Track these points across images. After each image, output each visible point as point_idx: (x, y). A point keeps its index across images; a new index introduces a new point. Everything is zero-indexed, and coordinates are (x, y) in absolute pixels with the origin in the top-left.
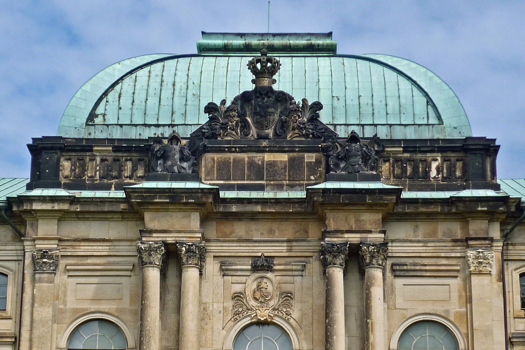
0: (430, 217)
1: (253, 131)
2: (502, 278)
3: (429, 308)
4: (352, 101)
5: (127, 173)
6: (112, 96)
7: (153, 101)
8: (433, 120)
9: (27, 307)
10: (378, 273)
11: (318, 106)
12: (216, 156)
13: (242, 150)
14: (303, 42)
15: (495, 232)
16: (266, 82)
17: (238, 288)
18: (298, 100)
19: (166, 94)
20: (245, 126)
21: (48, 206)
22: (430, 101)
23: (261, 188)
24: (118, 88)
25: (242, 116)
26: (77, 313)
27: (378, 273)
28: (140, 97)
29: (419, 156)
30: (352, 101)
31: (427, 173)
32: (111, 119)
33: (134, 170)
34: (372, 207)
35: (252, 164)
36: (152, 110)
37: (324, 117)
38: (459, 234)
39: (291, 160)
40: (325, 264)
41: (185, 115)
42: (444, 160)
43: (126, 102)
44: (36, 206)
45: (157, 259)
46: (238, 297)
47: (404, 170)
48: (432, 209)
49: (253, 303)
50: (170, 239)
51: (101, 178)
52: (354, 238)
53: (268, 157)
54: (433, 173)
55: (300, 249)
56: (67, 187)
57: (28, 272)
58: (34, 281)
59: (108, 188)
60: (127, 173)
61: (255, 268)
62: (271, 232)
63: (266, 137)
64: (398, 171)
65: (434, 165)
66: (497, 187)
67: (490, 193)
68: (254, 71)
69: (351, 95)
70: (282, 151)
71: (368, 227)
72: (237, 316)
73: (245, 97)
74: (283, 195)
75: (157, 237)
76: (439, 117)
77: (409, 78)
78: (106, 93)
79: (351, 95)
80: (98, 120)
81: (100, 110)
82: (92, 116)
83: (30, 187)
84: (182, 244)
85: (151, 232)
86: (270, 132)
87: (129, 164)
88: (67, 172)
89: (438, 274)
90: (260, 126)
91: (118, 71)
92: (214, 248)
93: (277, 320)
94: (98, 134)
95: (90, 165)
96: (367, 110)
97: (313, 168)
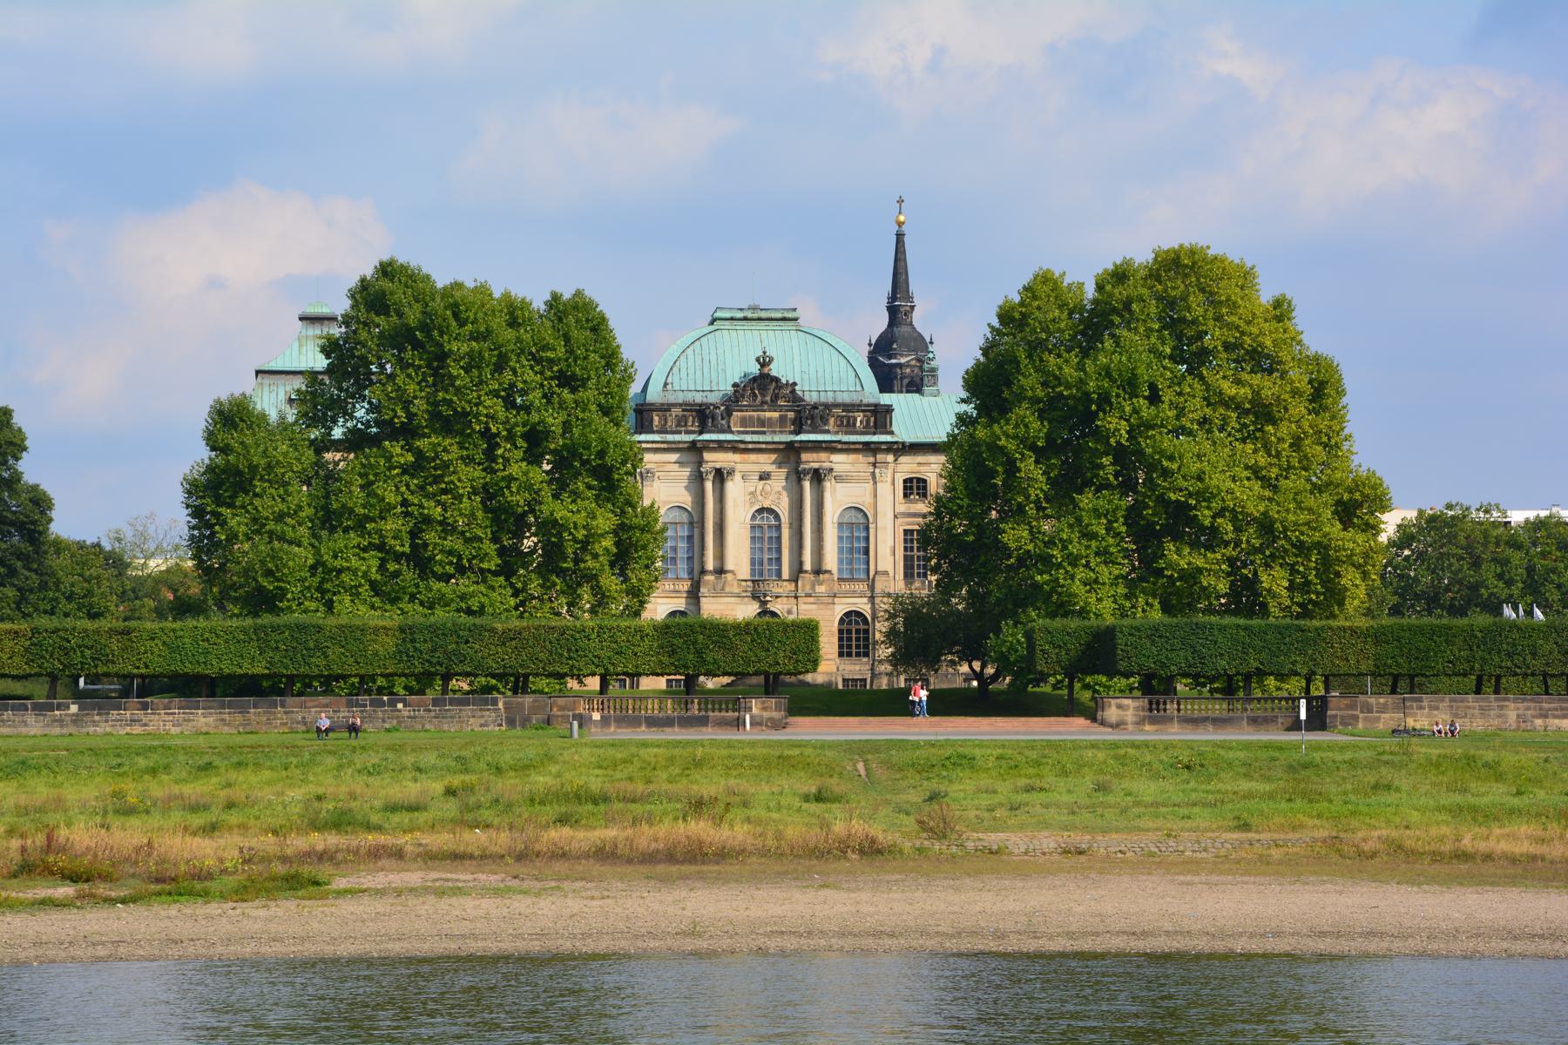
0: (856, 451)
1: (759, 398)
4: (813, 376)
5: (690, 424)
7: (699, 373)
8: (859, 388)
11: (795, 384)
13: (753, 411)
16: (766, 370)
17: (753, 489)
18: (784, 381)
20: (755, 395)
22: (857, 375)
23: (764, 433)
24: (678, 363)
25: (752, 389)
29: (851, 414)
31: (854, 424)
33: (693, 422)
35: (759, 418)
37: (797, 388)
39: (781, 417)
42: (864, 416)
44: (644, 445)
45: (711, 477)
46: (752, 493)
47: (842, 422)
48: (857, 446)
49: (760, 498)
51: (676, 426)
52: (816, 465)
53: (768, 414)
54: (858, 424)
56: (659, 432)
59: (680, 433)
60: (690, 424)
61: (761, 478)
63: (766, 403)
64: (839, 423)
65: (859, 419)
66: (892, 433)
67: (888, 438)
68: (759, 363)
69: (812, 372)
70: (775, 411)
72: (752, 504)
73: (755, 379)
74: (777, 438)
75: (710, 465)
78: (671, 369)
80: (669, 387)
81: (669, 380)
82: (666, 384)
86: (768, 398)
90: (763, 395)
91: (675, 350)
94: (671, 399)
95: (669, 419)
96: (821, 380)
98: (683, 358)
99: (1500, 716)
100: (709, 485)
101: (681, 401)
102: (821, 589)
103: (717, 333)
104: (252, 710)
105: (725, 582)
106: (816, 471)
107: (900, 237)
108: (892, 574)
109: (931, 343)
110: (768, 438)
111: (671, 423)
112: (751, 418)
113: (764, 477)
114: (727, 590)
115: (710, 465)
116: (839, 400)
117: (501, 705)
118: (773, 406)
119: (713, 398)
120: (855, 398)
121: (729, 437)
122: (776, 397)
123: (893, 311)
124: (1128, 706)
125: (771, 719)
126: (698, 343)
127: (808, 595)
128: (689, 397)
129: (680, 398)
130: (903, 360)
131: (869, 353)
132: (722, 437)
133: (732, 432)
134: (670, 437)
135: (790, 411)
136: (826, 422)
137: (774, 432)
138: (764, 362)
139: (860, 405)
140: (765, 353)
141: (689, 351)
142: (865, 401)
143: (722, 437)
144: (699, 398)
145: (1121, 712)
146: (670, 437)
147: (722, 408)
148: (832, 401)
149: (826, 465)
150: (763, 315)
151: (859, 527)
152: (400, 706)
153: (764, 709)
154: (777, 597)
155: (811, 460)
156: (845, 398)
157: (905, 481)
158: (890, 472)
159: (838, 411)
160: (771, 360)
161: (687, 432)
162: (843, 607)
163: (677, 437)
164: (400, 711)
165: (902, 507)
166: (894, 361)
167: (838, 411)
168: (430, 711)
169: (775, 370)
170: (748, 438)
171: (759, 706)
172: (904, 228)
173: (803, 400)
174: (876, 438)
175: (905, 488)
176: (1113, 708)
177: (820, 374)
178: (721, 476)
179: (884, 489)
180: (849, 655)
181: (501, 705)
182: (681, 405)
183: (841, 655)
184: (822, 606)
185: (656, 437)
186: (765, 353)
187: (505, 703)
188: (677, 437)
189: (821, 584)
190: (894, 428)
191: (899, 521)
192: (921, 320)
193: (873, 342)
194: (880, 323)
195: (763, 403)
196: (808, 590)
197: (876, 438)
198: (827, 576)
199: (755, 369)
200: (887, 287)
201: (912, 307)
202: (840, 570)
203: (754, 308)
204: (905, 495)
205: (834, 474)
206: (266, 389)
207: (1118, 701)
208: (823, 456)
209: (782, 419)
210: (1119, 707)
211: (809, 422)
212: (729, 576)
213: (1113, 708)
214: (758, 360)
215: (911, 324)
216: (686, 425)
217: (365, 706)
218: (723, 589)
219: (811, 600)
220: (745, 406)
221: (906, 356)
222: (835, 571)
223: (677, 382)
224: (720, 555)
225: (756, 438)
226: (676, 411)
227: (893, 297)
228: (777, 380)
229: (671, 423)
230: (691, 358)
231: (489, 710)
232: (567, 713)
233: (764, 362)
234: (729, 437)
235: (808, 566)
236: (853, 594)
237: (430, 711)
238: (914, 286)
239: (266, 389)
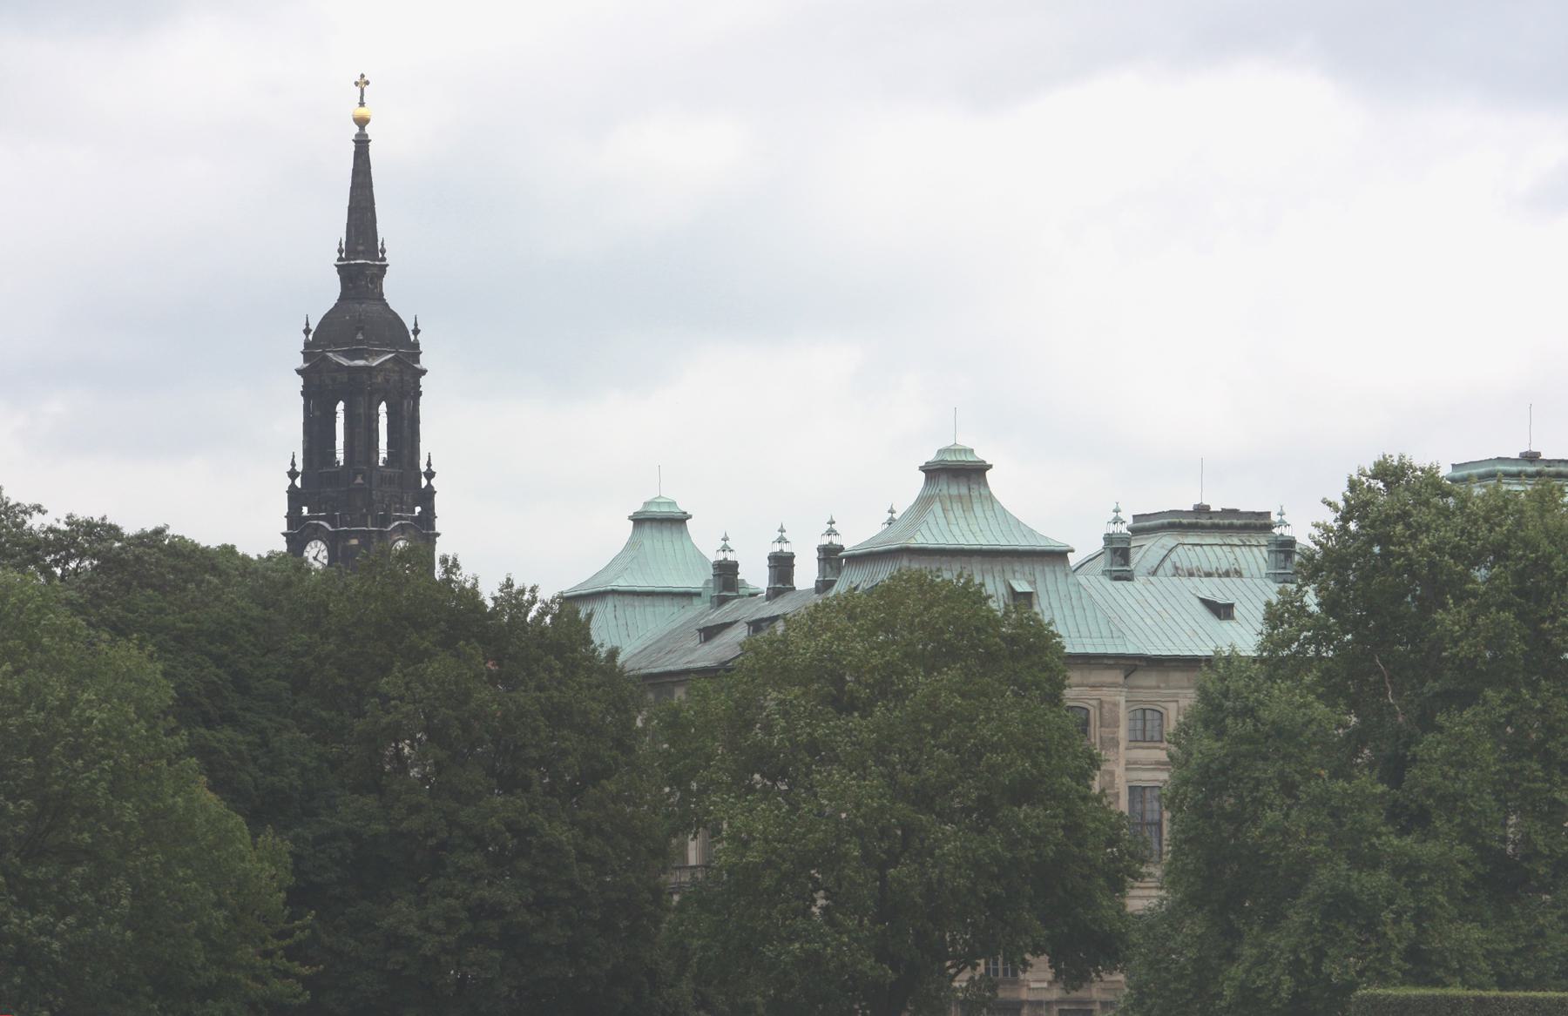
107: (362, 145)
109: (416, 332)
131: (307, 344)
166: (361, 363)
172: (368, 129)
192: (398, 292)
193: (313, 327)
194: (327, 291)
200: (338, 229)
201: (383, 269)
221: (379, 354)
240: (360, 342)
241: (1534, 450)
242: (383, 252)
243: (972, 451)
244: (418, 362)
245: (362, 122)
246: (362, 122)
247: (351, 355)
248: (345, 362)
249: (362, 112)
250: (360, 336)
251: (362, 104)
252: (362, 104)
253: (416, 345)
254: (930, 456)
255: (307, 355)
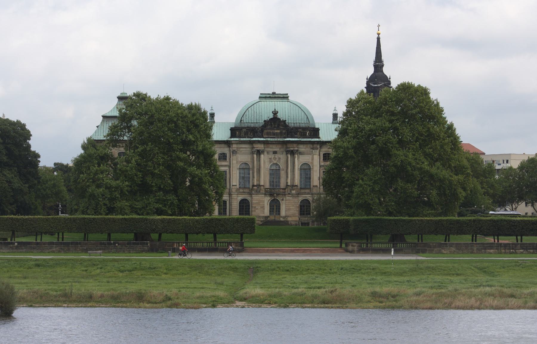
0: (306, 144)
1: (273, 126)
2: (319, 155)
3: (306, 161)
6: (245, 116)
7: (253, 117)
8: (308, 122)
9: (231, 161)
10: (296, 156)
11: (285, 121)
12: (266, 131)
13: (271, 130)
14: (282, 96)
15: (318, 147)
16: (275, 116)
17: (270, 157)
18: (282, 119)
19: (255, 115)
21: (235, 142)
22: (307, 118)
23: (274, 138)
24: (245, 113)
25: (271, 123)
26: (241, 162)
27: (296, 156)
28: (250, 116)
29: (305, 131)
30: (292, 118)
32: (245, 122)
33: (250, 134)
34: (295, 143)
36: (253, 119)
37: (287, 122)
38: (312, 147)
39: (280, 132)
40: (287, 154)
41: (259, 120)
43: (247, 117)
44: (233, 142)
45: (256, 153)
46: (270, 159)
49: (273, 160)
50: (258, 149)
51: (244, 135)
52: (292, 149)
53: (276, 131)
54: (307, 134)
55: (282, 150)
57: (231, 154)
58: (233, 156)
59: (245, 137)
62: (277, 146)
65: (308, 133)
66: (319, 138)
67: (317, 140)
69: (292, 116)
70: (279, 130)
71: (295, 147)
74: (279, 140)
75: (255, 149)
76: (309, 121)
77: (304, 111)
78: (243, 115)
79: (292, 116)
80: (242, 122)
81: (242, 119)
82: (241, 121)
83: (231, 137)
84: (260, 150)
85: (255, 148)
86: (276, 126)
87: (249, 132)
88: (237, 134)
89: (308, 154)
92: (266, 149)
93: (278, 163)
94: (243, 125)
97: (285, 133)
98: (247, 112)
99: (471, 249)
100: (255, 156)
101: (246, 126)
102: (294, 192)
103: (259, 102)
104: (70, 245)
105: (260, 190)
106: (292, 151)
107: (378, 39)
108: (319, 186)
109: (390, 79)
110: (276, 139)
111: (243, 134)
112: (270, 132)
113: (275, 153)
114: (261, 192)
115: (255, 149)
116: (301, 126)
117: (149, 245)
118: (278, 128)
119: (257, 125)
120: (307, 125)
121: (262, 139)
122: (279, 125)
123: (376, 67)
124: (355, 245)
125: (239, 249)
126: (253, 106)
127: (289, 194)
128: (249, 125)
129: (246, 125)
130: (379, 85)
131: (367, 82)
132: (260, 139)
133: (264, 138)
134: (242, 139)
135: (284, 130)
136: (297, 134)
137: (278, 137)
138: (275, 113)
139: (308, 128)
140: (275, 110)
141: (250, 109)
142: (310, 126)
143: (260, 139)
144: (252, 125)
145: (353, 248)
146: (242, 139)
147: (260, 129)
148: (298, 126)
149: (296, 149)
150: (276, 96)
151: (306, 170)
152: (117, 245)
153: (236, 246)
154: (278, 194)
155: (292, 148)
156: (303, 125)
157: (324, 154)
158: (318, 151)
159: (300, 130)
160: (278, 112)
161: (248, 137)
162: (302, 198)
163: (244, 139)
164: (117, 246)
165: (322, 164)
166: (376, 85)
167: (300, 130)
168: (126, 246)
169: (279, 116)
170: (269, 139)
171: (235, 245)
172: (380, 36)
173: (288, 126)
174: (313, 140)
175: (324, 157)
176: (350, 246)
177: (295, 117)
178: (259, 153)
179: (316, 157)
180: (304, 214)
181: (149, 245)
182: (246, 128)
183: (301, 214)
184: (294, 198)
185: (237, 139)
186: (275, 110)
187: (150, 244)
188: (244, 139)
189: (294, 190)
190: (321, 135)
191: (322, 168)
192: (387, 71)
193: (368, 78)
194: (371, 71)
195: (275, 127)
196: (289, 192)
197: (313, 140)
198: (296, 187)
199: (271, 116)
201: (383, 65)
202: (301, 185)
203: (274, 93)
204: (323, 159)
205: (299, 152)
206: (105, 122)
207: (352, 244)
208: (295, 145)
209: (281, 133)
210: (352, 246)
211: (290, 134)
212: (262, 187)
213: (350, 246)
214: (273, 112)
215: (382, 71)
216: (248, 135)
217: (106, 245)
218: (260, 192)
219: (290, 196)
220: (268, 128)
221: (381, 83)
222: (299, 185)
223: (244, 119)
224: (259, 180)
225: (272, 139)
226: (244, 130)
227: (376, 62)
228: (279, 119)
229: (243, 134)
230: (250, 111)
231: (145, 246)
232: (170, 248)
233: (275, 113)
234: (262, 139)
235: (289, 184)
236: (305, 193)
237: (126, 246)
238: (383, 58)
239: (105, 122)
240: (376, 81)
241: (275, 92)
242: (383, 61)
243: (126, 94)
244: (390, 85)
245: (379, 34)
246: (379, 34)
247: (374, 84)
248: (373, 85)
249: (379, 32)
250: (376, 80)
251: (379, 30)
252: (379, 30)
253: (390, 81)
254: (119, 94)
255: (367, 84)
